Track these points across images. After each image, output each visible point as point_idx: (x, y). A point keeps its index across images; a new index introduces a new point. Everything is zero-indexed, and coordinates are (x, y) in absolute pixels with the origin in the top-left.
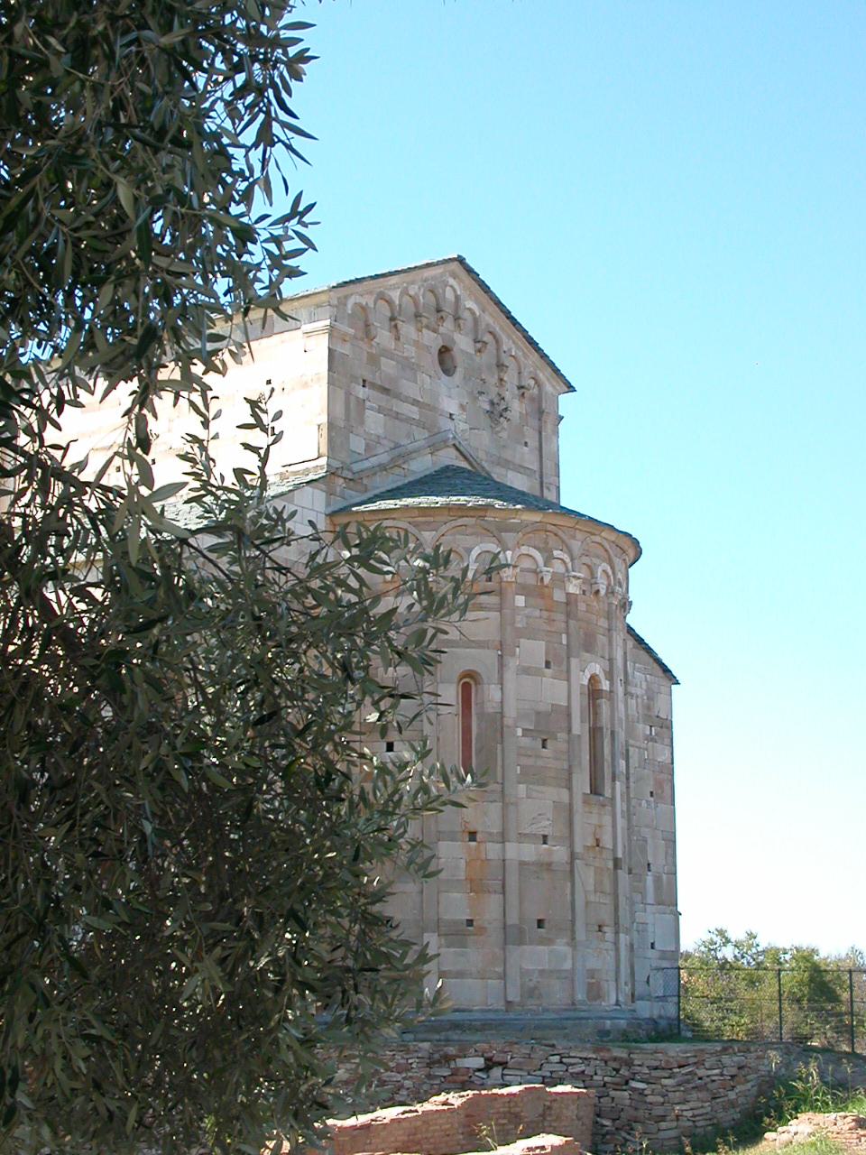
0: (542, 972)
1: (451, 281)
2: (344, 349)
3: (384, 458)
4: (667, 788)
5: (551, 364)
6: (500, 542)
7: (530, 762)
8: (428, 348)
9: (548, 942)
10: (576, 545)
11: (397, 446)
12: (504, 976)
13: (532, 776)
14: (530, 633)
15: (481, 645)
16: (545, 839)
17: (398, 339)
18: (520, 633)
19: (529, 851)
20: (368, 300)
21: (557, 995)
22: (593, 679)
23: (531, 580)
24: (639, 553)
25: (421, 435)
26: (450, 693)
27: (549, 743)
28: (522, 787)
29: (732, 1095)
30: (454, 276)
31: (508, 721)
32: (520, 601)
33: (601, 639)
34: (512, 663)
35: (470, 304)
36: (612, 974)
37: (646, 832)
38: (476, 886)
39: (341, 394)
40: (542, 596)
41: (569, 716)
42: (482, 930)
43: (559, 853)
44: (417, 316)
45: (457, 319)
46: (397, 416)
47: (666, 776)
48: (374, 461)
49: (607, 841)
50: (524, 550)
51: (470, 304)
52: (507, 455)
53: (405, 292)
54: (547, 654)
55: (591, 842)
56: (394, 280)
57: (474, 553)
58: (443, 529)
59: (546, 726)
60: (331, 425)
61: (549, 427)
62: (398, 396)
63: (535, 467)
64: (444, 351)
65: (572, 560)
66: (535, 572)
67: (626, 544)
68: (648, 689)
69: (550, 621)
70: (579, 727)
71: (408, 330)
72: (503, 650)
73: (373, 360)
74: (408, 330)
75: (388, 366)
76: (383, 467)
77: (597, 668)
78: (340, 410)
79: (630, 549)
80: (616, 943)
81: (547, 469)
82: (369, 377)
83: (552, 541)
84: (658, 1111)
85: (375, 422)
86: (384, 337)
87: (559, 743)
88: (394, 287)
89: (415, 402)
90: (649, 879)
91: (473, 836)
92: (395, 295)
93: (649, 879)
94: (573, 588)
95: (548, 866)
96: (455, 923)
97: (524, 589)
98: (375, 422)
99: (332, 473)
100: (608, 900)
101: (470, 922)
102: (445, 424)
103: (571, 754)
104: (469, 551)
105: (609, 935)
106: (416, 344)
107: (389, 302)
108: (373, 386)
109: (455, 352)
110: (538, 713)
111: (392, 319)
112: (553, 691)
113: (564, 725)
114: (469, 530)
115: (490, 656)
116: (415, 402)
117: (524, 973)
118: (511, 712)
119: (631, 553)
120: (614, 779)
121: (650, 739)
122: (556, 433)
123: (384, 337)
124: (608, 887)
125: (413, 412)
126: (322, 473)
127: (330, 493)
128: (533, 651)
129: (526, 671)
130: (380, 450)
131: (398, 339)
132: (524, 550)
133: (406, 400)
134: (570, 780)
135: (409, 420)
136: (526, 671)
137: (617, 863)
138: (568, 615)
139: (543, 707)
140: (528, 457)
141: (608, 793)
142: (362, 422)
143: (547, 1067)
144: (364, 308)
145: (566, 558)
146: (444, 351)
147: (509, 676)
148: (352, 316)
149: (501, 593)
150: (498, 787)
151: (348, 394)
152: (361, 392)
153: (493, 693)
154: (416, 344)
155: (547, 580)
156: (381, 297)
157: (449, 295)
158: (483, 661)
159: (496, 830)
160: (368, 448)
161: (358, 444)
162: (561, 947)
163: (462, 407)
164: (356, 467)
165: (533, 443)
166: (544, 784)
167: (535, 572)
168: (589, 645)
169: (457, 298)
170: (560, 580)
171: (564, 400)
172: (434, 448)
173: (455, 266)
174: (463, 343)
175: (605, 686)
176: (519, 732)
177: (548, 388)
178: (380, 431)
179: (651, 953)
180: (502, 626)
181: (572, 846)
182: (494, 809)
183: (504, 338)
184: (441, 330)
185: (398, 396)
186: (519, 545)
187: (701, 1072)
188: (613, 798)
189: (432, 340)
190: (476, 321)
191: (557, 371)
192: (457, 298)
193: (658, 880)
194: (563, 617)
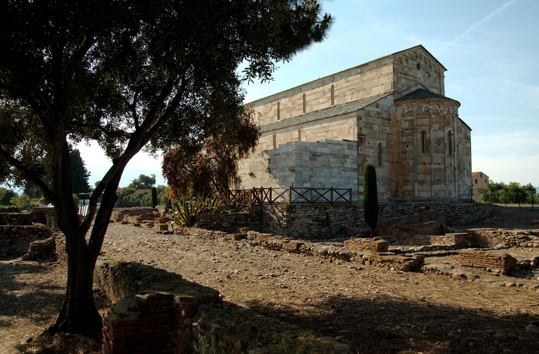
0: (439, 190)
1: (419, 50)
2: (396, 67)
3: (406, 88)
4: (469, 152)
5: (442, 65)
7: (436, 148)
8: (414, 65)
9: (440, 184)
10: (445, 104)
11: (408, 85)
12: (431, 191)
13: (437, 151)
14: (436, 123)
15: (426, 125)
16: (439, 164)
17: (408, 63)
18: (434, 123)
19: (436, 166)
20: (401, 56)
21: (442, 195)
22: (450, 131)
23: (436, 112)
24: (460, 105)
25: (413, 83)
26: (419, 136)
28: (434, 154)
29: (476, 214)
30: (420, 49)
31: (431, 141)
32: (433, 116)
33: (451, 123)
34: (432, 129)
35: (423, 54)
36: (454, 190)
37: (465, 161)
38: (425, 173)
39: (396, 76)
40: (438, 115)
41: (444, 139)
42: (426, 182)
43: (442, 167)
44: (412, 58)
45: (421, 58)
46: (408, 79)
47: (469, 150)
48: (403, 89)
49: (453, 164)
50: (434, 106)
51: (423, 54)
52: (432, 85)
53: (409, 54)
55: (449, 164)
56: (406, 51)
57: (424, 107)
58: (417, 102)
59: (439, 141)
60: (394, 82)
61: (442, 78)
62: (408, 75)
63: (439, 87)
67: (457, 103)
68: (465, 132)
69: (440, 120)
70: (446, 141)
71: (410, 61)
72: (430, 126)
73: (403, 68)
74: (410, 61)
75: (406, 69)
76: (405, 90)
77: (450, 129)
78: (396, 79)
79: (458, 104)
80: (455, 184)
81: (441, 88)
82: (402, 72)
83: (440, 103)
84: (460, 217)
85: (403, 81)
86: (405, 63)
87: (442, 145)
88: (406, 53)
89: (412, 76)
90: (465, 171)
91: (424, 164)
92: (407, 54)
93: (465, 171)
94: (445, 113)
95: (440, 169)
96: (421, 181)
97: (434, 114)
98: (403, 81)
99: (394, 92)
100: (453, 176)
101: (424, 181)
102: (418, 80)
103: (445, 147)
104: (423, 106)
105: (453, 183)
106: (412, 64)
107: (406, 56)
108: (403, 74)
109: (420, 65)
111: (406, 59)
112: (441, 134)
115: (427, 128)
116: (412, 76)
117: (435, 190)
118: (432, 139)
119: (458, 105)
120: (454, 151)
121: (465, 142)
122: (443, 80)
123: (405, 63)
124: (453, 173)
125: (412, 78)
126: (392, 92)
127: (394, 96)
128: (436, 126)
129: (435, 130)
130: (404, 87)
131: (408, 63)
132: (434, 106)
133: (410, 76)
134: (445, 152)
135: (411, 80)
136: (435, 130)
137: (455, 168)
138: (444, 119)
139: (439, 137)
140: (437, 85)
141: (453, 154)
142: (401, 81)
143: (438, 208)
144: (400, 58)
145: (443, 107)
147: (431, 131)
148: (398, 59)
149: (429, 115)
150: (429, 154)
151: (397, 76)
152: (400, 75)
153: (428, 135)
154: (412, 64)
155: (439, 111)
156: (404, 55)
157: (419, 53)
158: (426, 129)
159: (429, 162)
160: (402, 86)
161: (400, 86)
162: (443, 185)
163: (422, 76)
164: (399, 91)
165: (438, 82)
166: (439, 153)
168: (448, 124)
169: (421, 53)
170: (442, 111)
171: (445, 73)
172: (416, 85)
173: (420, 47)
174: (422, 63)
175: (452, 132)
176: (434, 143)
177: (442, 70)
178: (405, 83)
179: (466, 186)
180: (430, 121)
181: (445, 165)
182: (429, 158)
183: (431, 61)
184: (417, 60)
185: (408, 75)
186: (433, 105)
187: (470, 209)
188: (454, 155)
189: (415, 63)
190: (425, 58)
191: (443, 67)
192: (421, 53)
193: (467, 171)
194: (443, 119)
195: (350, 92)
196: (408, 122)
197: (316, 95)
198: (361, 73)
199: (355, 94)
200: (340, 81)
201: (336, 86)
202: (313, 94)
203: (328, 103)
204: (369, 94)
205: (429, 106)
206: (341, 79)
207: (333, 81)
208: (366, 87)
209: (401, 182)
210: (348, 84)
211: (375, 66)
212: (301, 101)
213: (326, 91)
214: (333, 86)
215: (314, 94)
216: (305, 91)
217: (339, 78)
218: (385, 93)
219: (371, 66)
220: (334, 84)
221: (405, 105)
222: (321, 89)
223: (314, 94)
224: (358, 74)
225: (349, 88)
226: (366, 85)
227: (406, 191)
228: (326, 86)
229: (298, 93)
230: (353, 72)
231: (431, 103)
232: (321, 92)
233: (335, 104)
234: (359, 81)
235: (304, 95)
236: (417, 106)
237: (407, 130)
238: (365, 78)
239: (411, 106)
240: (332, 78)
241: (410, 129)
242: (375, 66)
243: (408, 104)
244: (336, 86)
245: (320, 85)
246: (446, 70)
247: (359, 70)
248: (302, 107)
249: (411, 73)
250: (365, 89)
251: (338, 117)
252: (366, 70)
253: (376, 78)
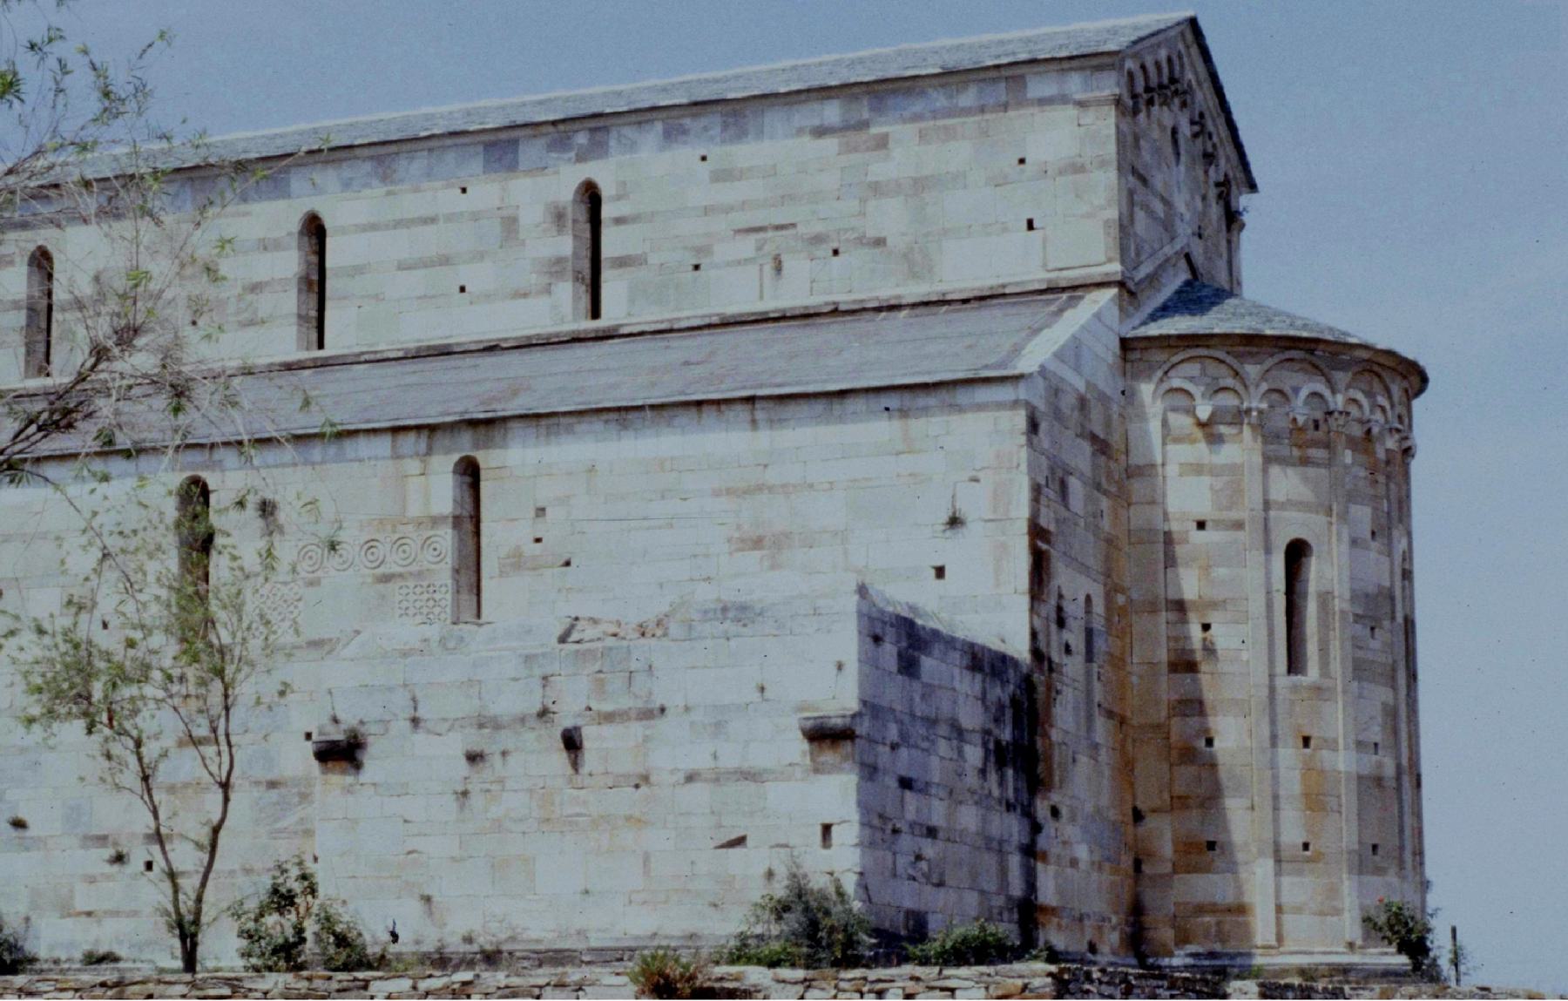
6: (1330, 383)
27: (1377, 630)
41: (1392, 599)
54: (1373, 520)
57: (1304, 393)
64: (1174, 131)
65: (1392, 406)
66: (1361, 422)
83: (1377, 386)
97: (1352, 443)
104: (1296, 390)
110: (1367, 595)
113: (1387, 609)
114: (1297, 366)
133: (1155, 193)
139: (1371, 589)
146: (1174, 131)
167: (1361, 422)
195: (747, 246)
196: (1206, 480)
203: (540, 304)
205: (1327, 393)
209: (1167, 850)
212: (290, 262)
221: (1193, 369)
224: (821, 132)
226: (890, 218)
227: (1200, 910)
231: (1341, 377)
236: (1264, 387)
237: (1201, 525)
238: (882, 169)
239: (1230, 382)
241: (1219, 524)
243: (1213, 368)
246: (1253, 187)
249: (1158, 181)
250: (880, 242)
251: (853, 404)
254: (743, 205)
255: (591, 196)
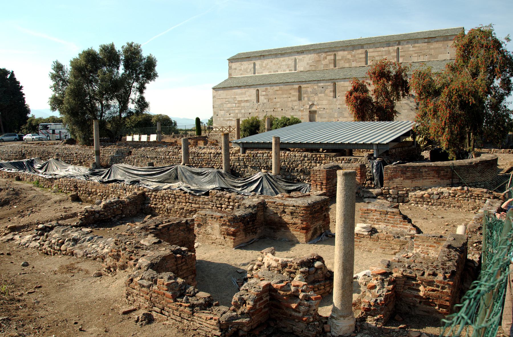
195: (416, 55)
197: (380, 52)
198: (428, 42)
199: (422, 57)
200: (407, 46)
201: (402, 49)
202: (376, 52)
204: (436, 58)
206: (407, 44)
207: (399, 44)
208: (433, 53)
210: (414, 49)
211: (442, 39)
212: (364, 56)
213: (391, 51)
214: (398, 49)
215: (378, 51)
216: (367, 48)
217: (405, 43)
218: (451, 59)
219: (438, 39)
220: (400, 47)
222: (386, 49)
223: (378, 51)
225: (416, 52)
226: (432, 52)
228: (390, 48)
229: (359, 49)
230: (420, 41)
232: (385, 51)
233: (400, 62)
234: (426, 48)
235: (366, 52)
238: (432, 47)
240: (397, 43)
242: (442, 39)
244: (402, 49)
245: (385, 46)
247: (426, 40)
248: (364, 60)
250: (431, 55)
252: (433, 41)
253: (443, 48)
254: (416, 50)
255: (398, 49)
